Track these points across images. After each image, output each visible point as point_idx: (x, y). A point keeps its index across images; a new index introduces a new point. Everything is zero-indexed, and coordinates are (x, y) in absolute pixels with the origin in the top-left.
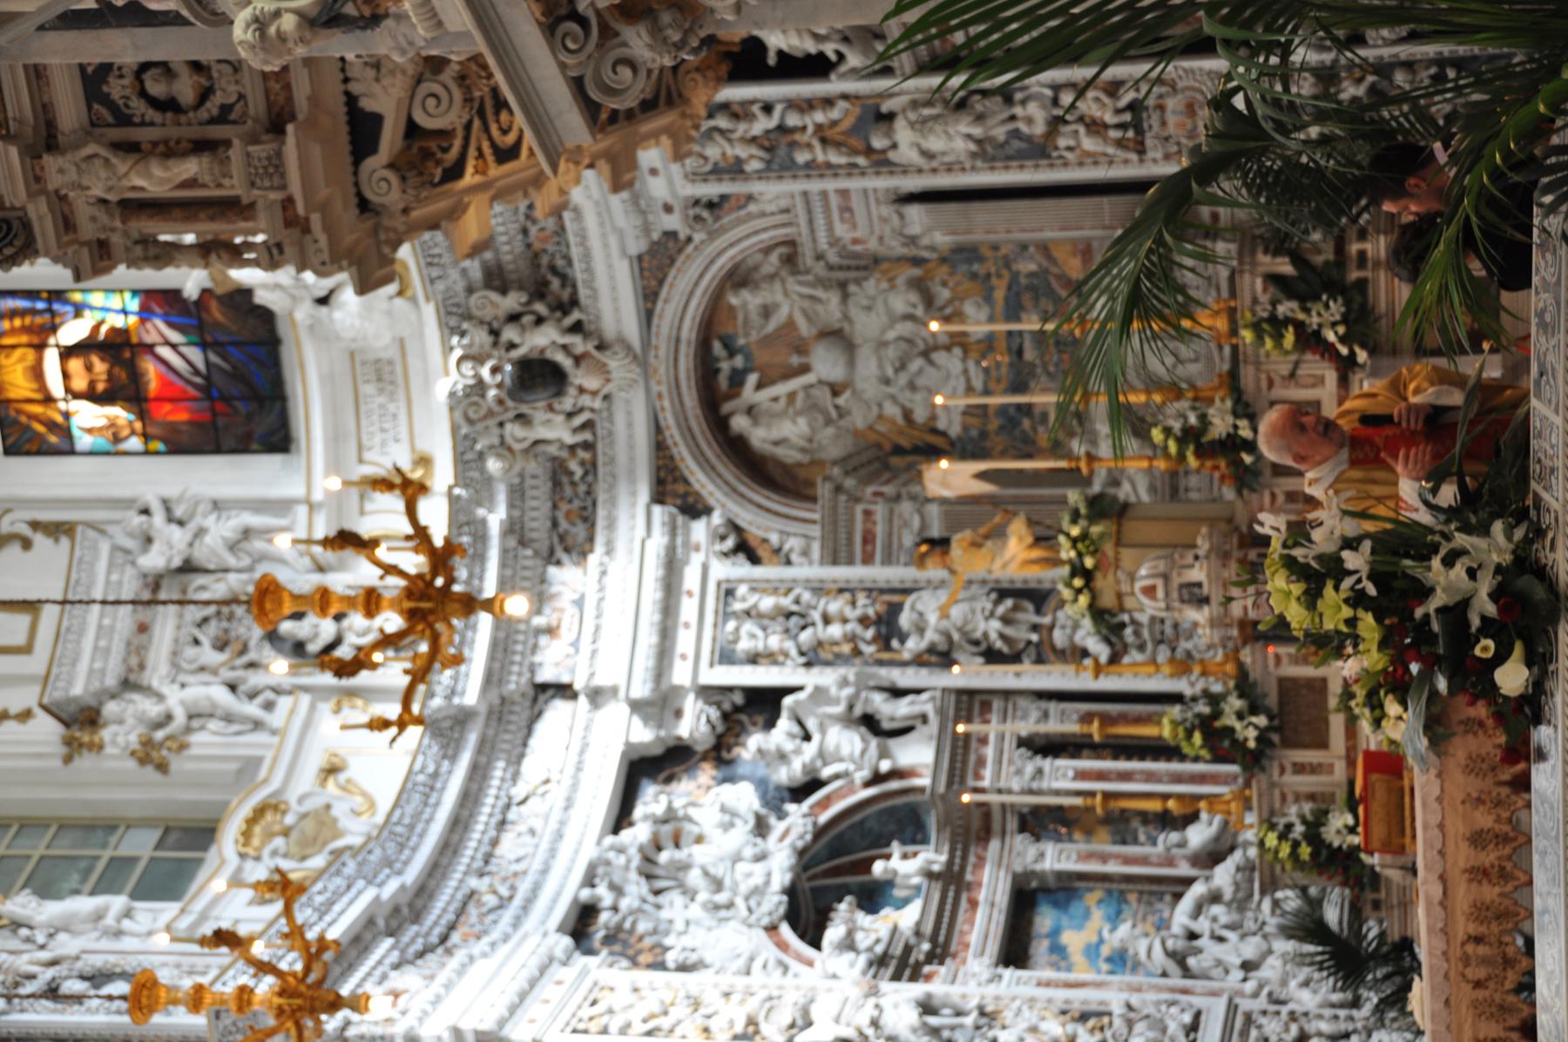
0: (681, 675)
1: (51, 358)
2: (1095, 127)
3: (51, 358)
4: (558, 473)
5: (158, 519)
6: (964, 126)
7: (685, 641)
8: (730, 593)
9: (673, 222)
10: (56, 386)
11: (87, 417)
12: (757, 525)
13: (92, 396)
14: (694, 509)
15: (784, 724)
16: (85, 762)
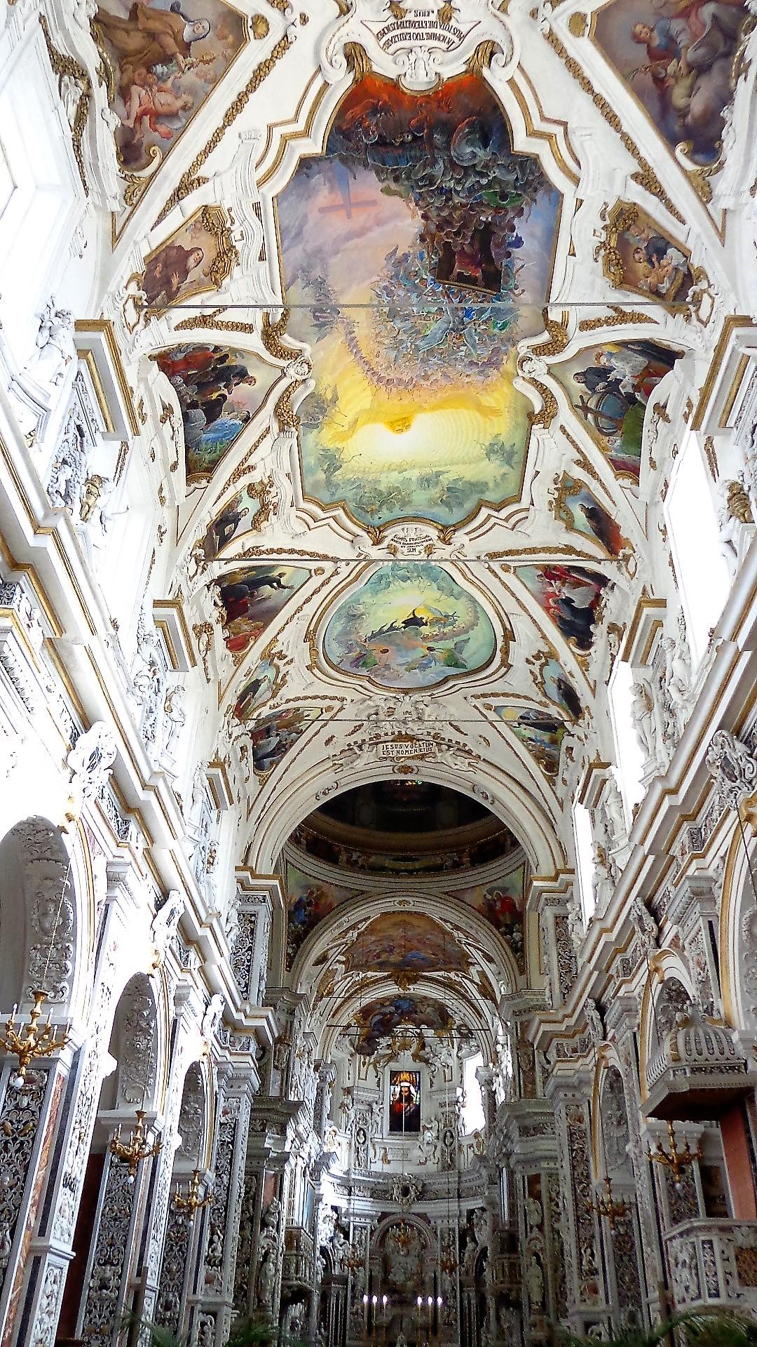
0: (352, 1219)
1: (408, 1084)
2: (448, 1315)
3: (408, 1084)
4: (386, 1192)
5: (381, 1106)
6: (450, 1288)
7: (358, 1219)
8: (365, 1229)
9: (432, 1223)
10: (402, 1084)
11: (398, 1090)
12: (376, 1234)
13: (401, 1091)
14: (379, 1221)
15: (342, 1240)
16: (342, 1091)
